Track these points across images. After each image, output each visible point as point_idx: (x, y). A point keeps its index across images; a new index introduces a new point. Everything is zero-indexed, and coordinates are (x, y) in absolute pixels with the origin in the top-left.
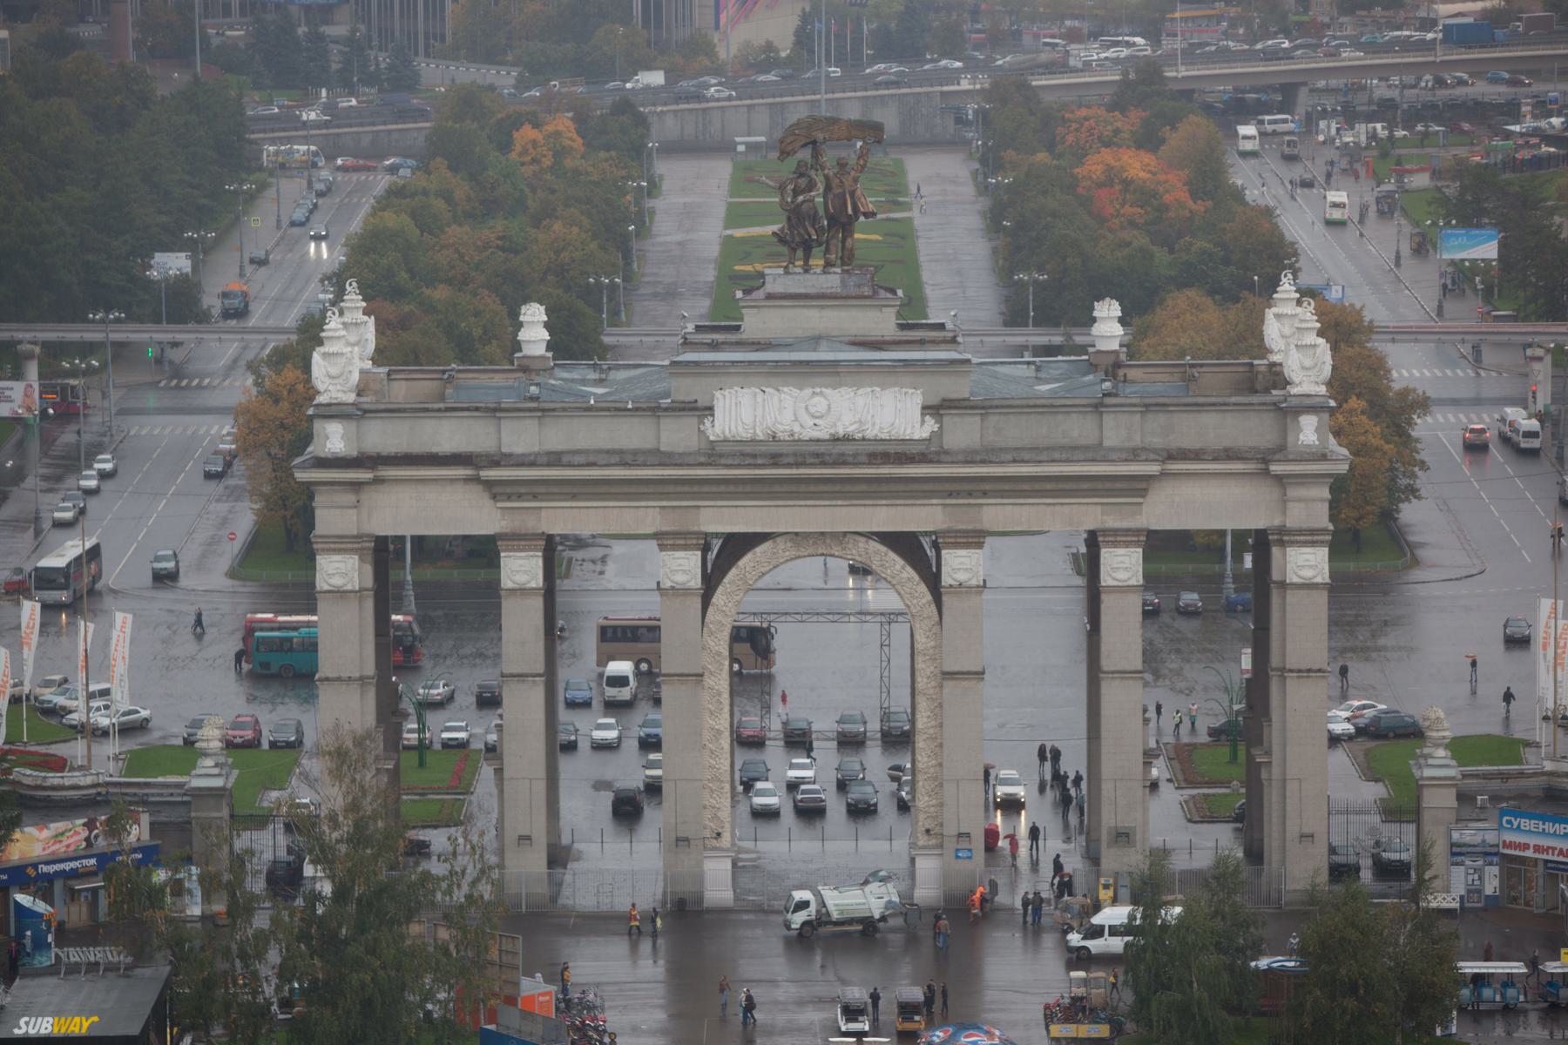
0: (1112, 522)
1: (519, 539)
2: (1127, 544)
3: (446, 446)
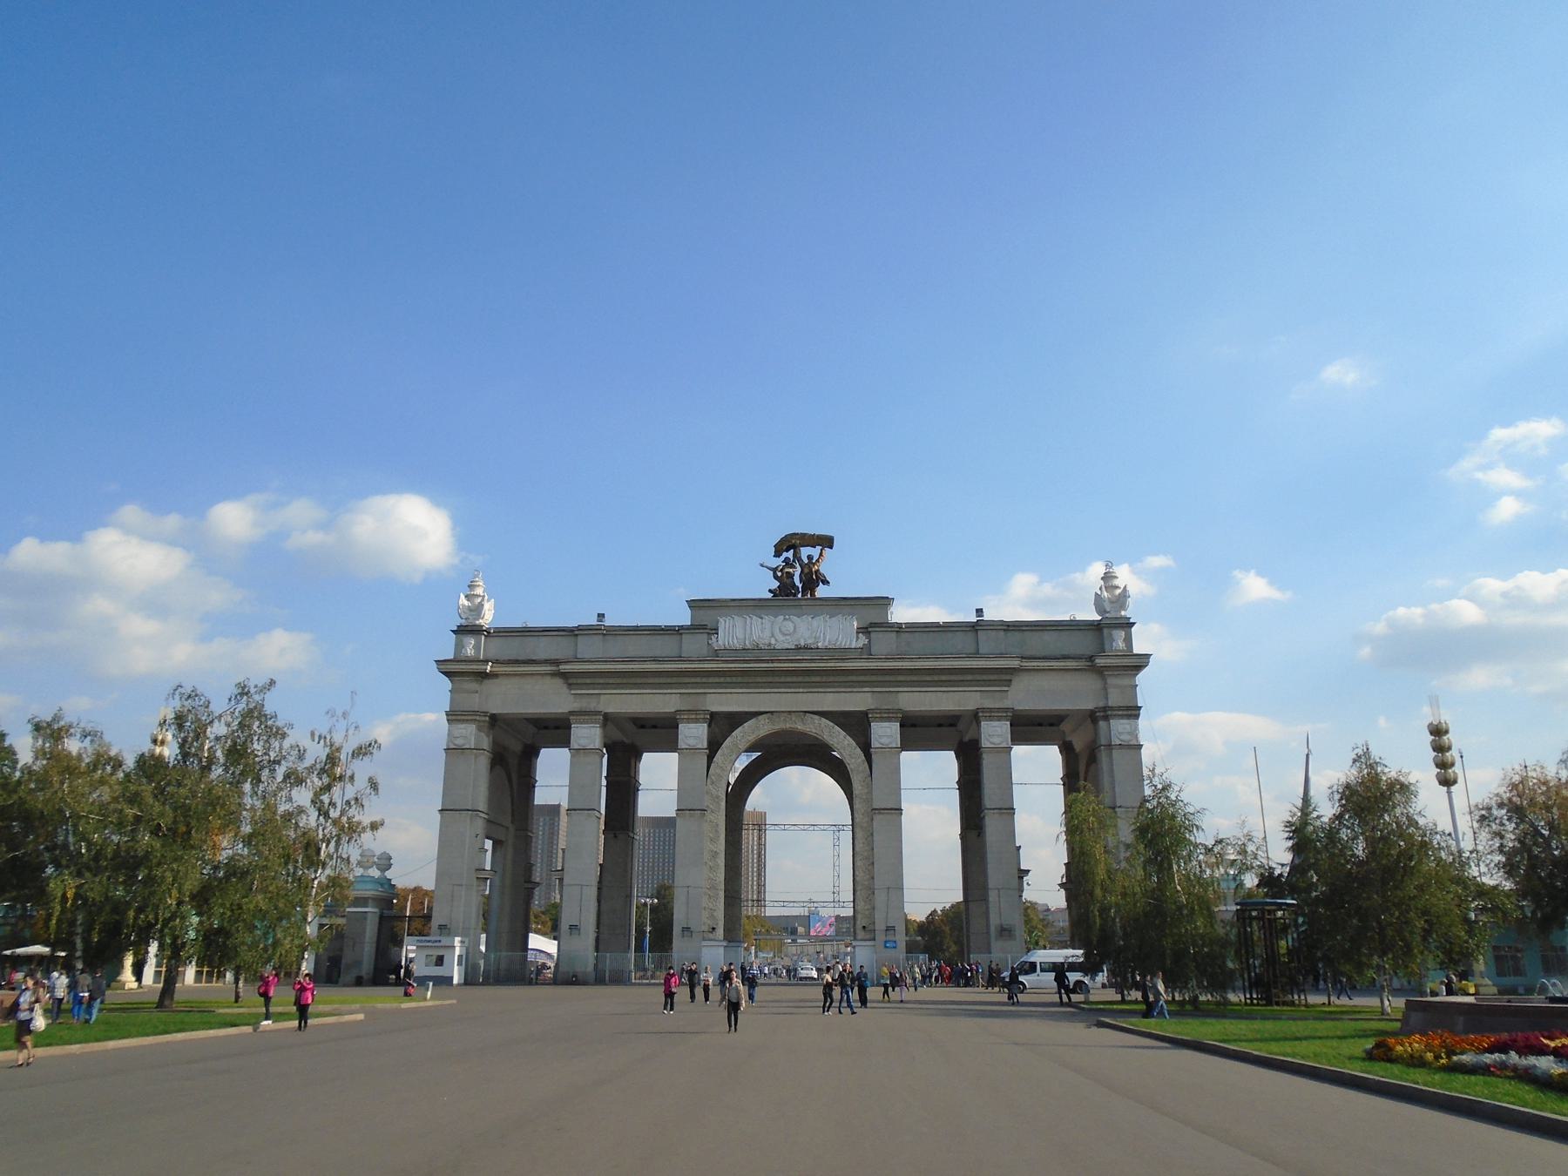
0: (988, 704)
1: (585, 715)
2: (999, 719)
3: (543, 656)
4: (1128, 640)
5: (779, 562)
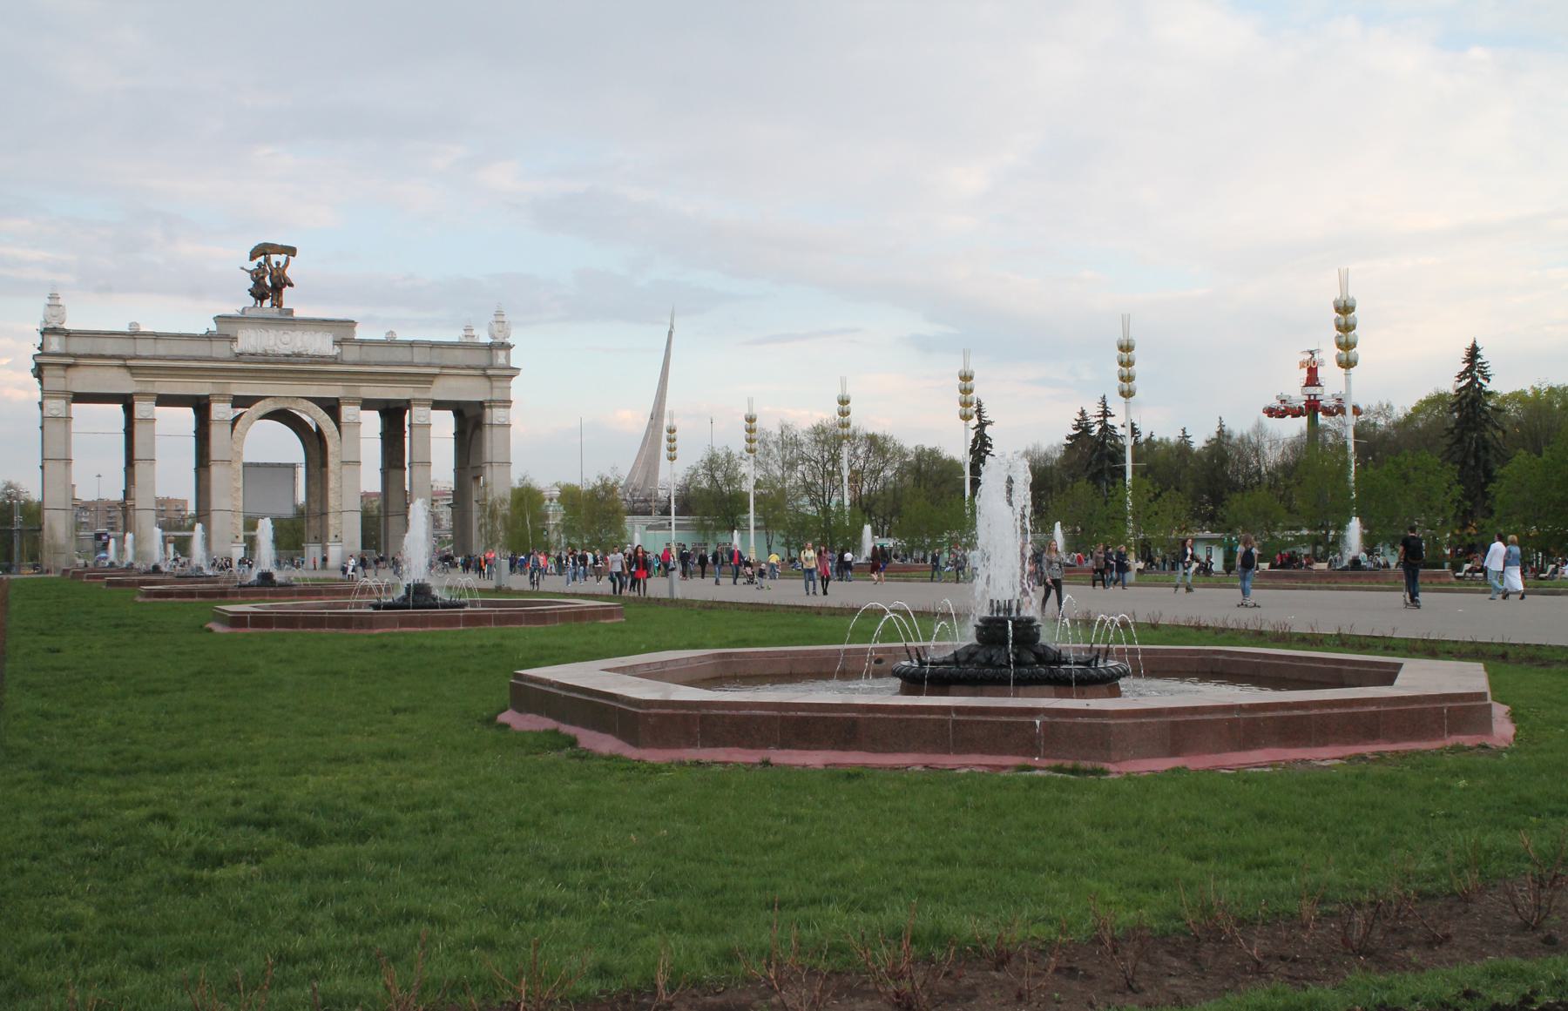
0: (417, 396)
3: (109, 352)
4: (508, 358)
5: (253, 265)
